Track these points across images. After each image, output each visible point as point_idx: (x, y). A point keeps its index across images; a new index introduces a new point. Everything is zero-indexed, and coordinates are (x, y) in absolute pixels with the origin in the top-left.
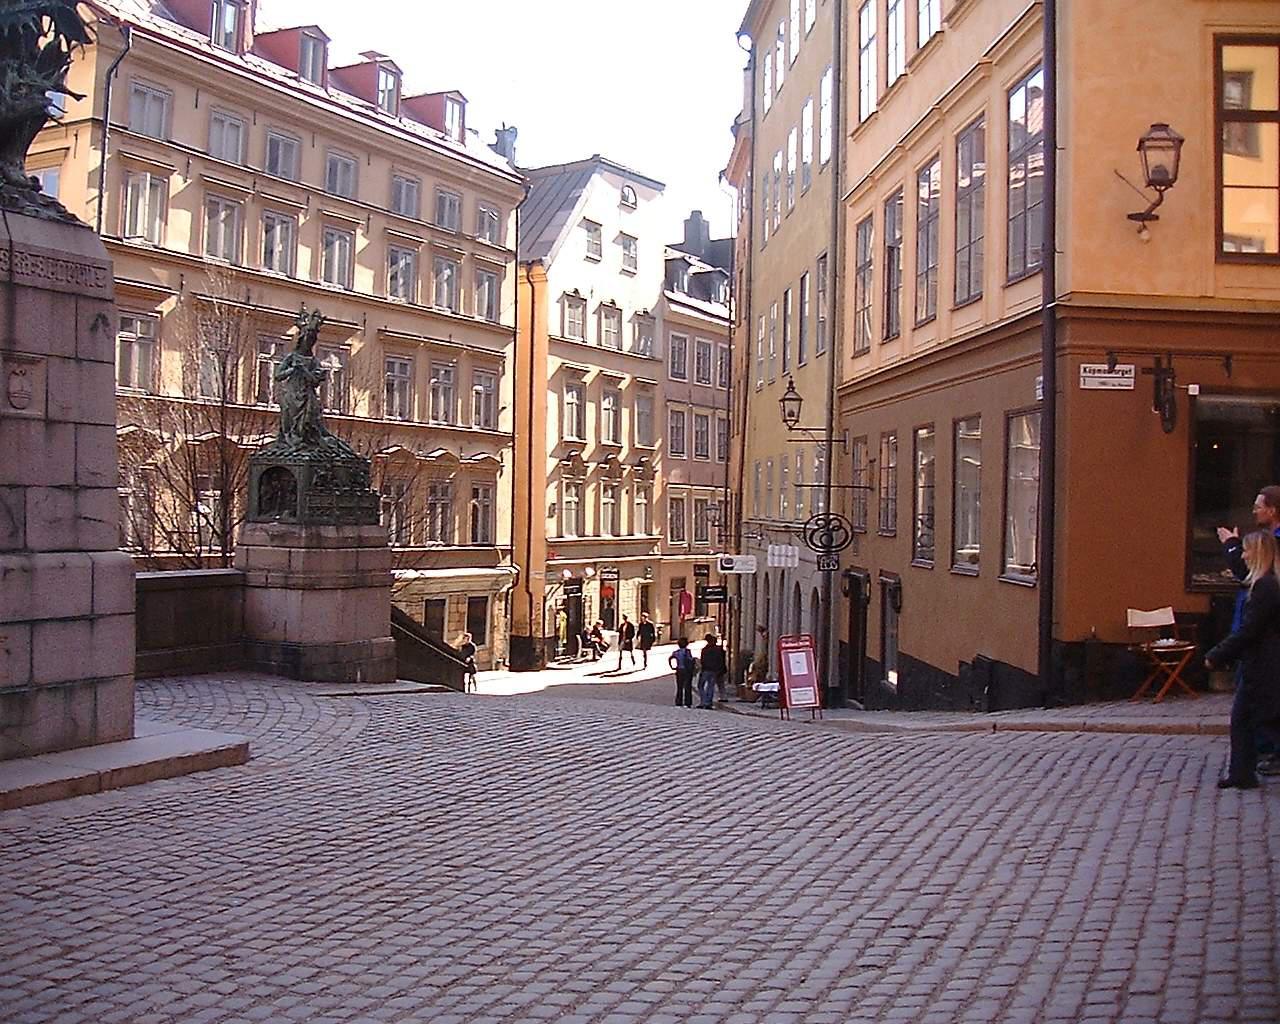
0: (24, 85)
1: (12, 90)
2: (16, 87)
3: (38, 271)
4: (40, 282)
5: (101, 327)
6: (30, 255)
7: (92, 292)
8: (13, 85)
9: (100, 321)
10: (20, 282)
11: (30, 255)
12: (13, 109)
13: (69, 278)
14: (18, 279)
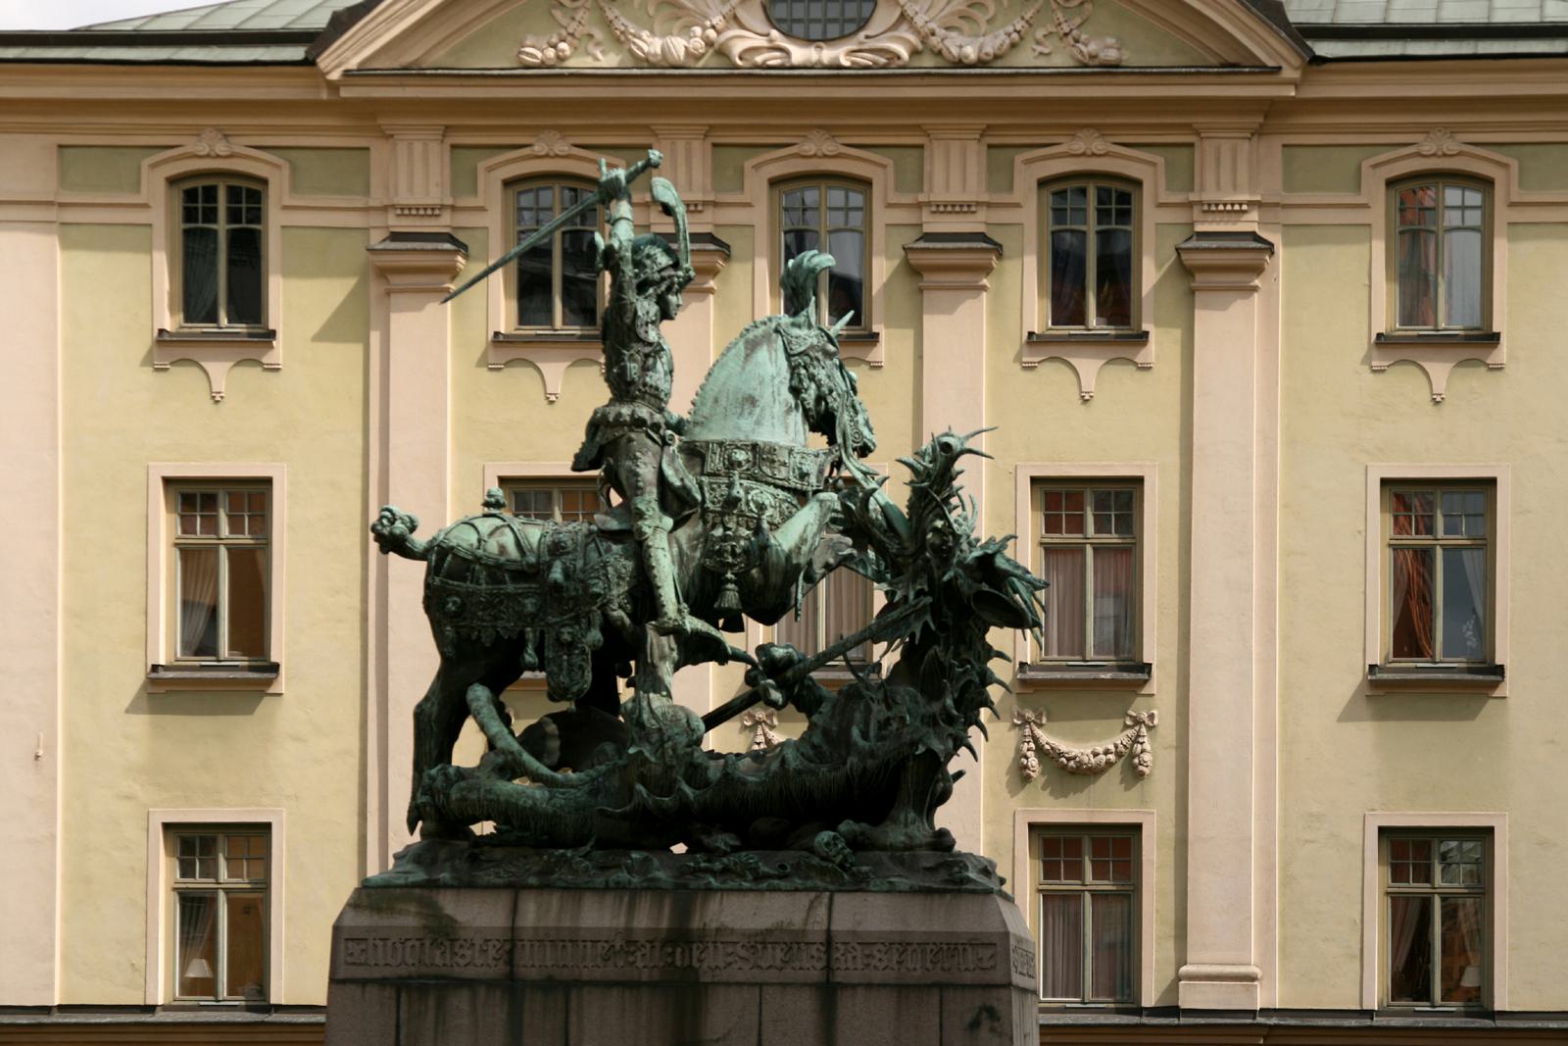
0: (894, 719)
1: (880, 729)
2: (884, 724)
3: (874, 962)
4: (877, 977)
5: (986, 1024)
6: (859, 943)
7: (968, 978)
8: (879, 722)
9: (984, 1015)
10: (844, 981)
11: (859, 943)
12: (872, 754)
13: (929, 965)
14: (839, 977)
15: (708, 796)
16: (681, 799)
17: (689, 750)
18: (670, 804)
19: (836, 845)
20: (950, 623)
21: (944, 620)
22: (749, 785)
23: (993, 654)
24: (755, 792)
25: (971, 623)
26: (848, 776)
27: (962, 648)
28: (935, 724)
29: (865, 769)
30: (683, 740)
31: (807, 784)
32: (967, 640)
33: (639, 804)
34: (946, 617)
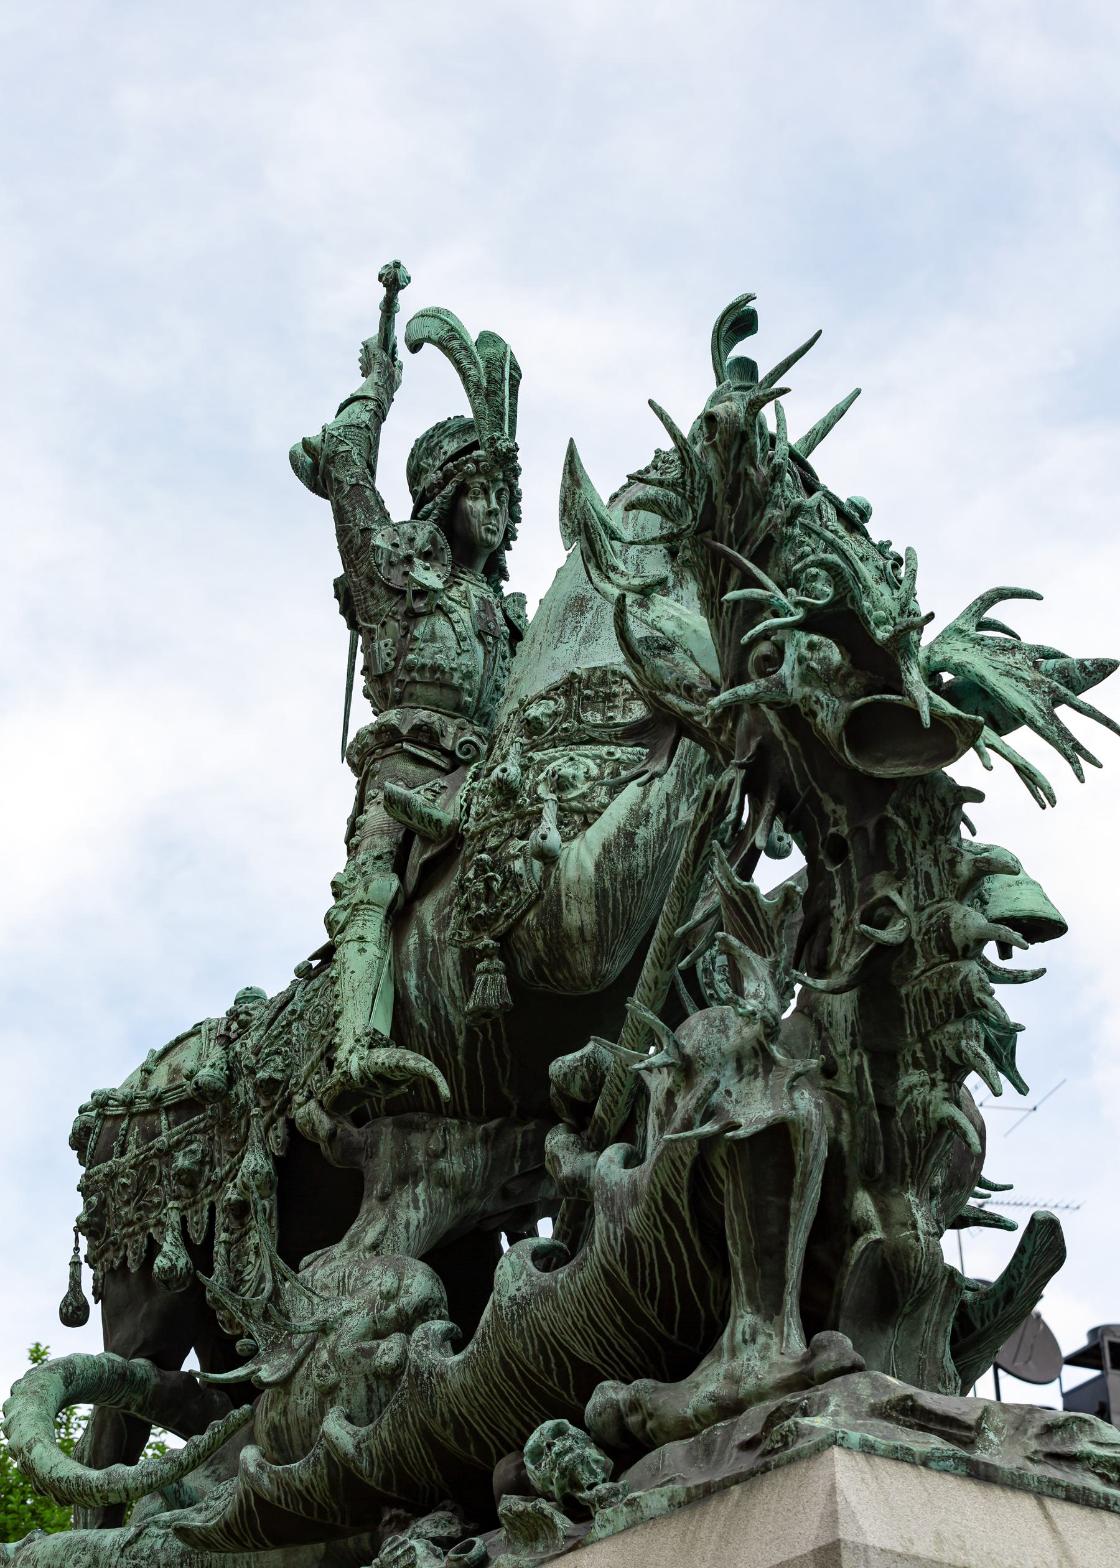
15: (385, 1434)
16: (327, 1454)
17: (375, 1342)
18: (305, 1476)
19: (550, 1446)
20: (844, 830)
21: (832, 830)
22: (449, 1376)
23: (964, 869)
24: (463, 1386)
25: (890, 812)
26: (602, 1265)
27: (879, 878)
28: (770, 1062)
29: (628, 1233)
30: (357, 1323)
31: (543, 1324)
32: (893, 857)
33: (246, 1493)
34: (836, 824)
